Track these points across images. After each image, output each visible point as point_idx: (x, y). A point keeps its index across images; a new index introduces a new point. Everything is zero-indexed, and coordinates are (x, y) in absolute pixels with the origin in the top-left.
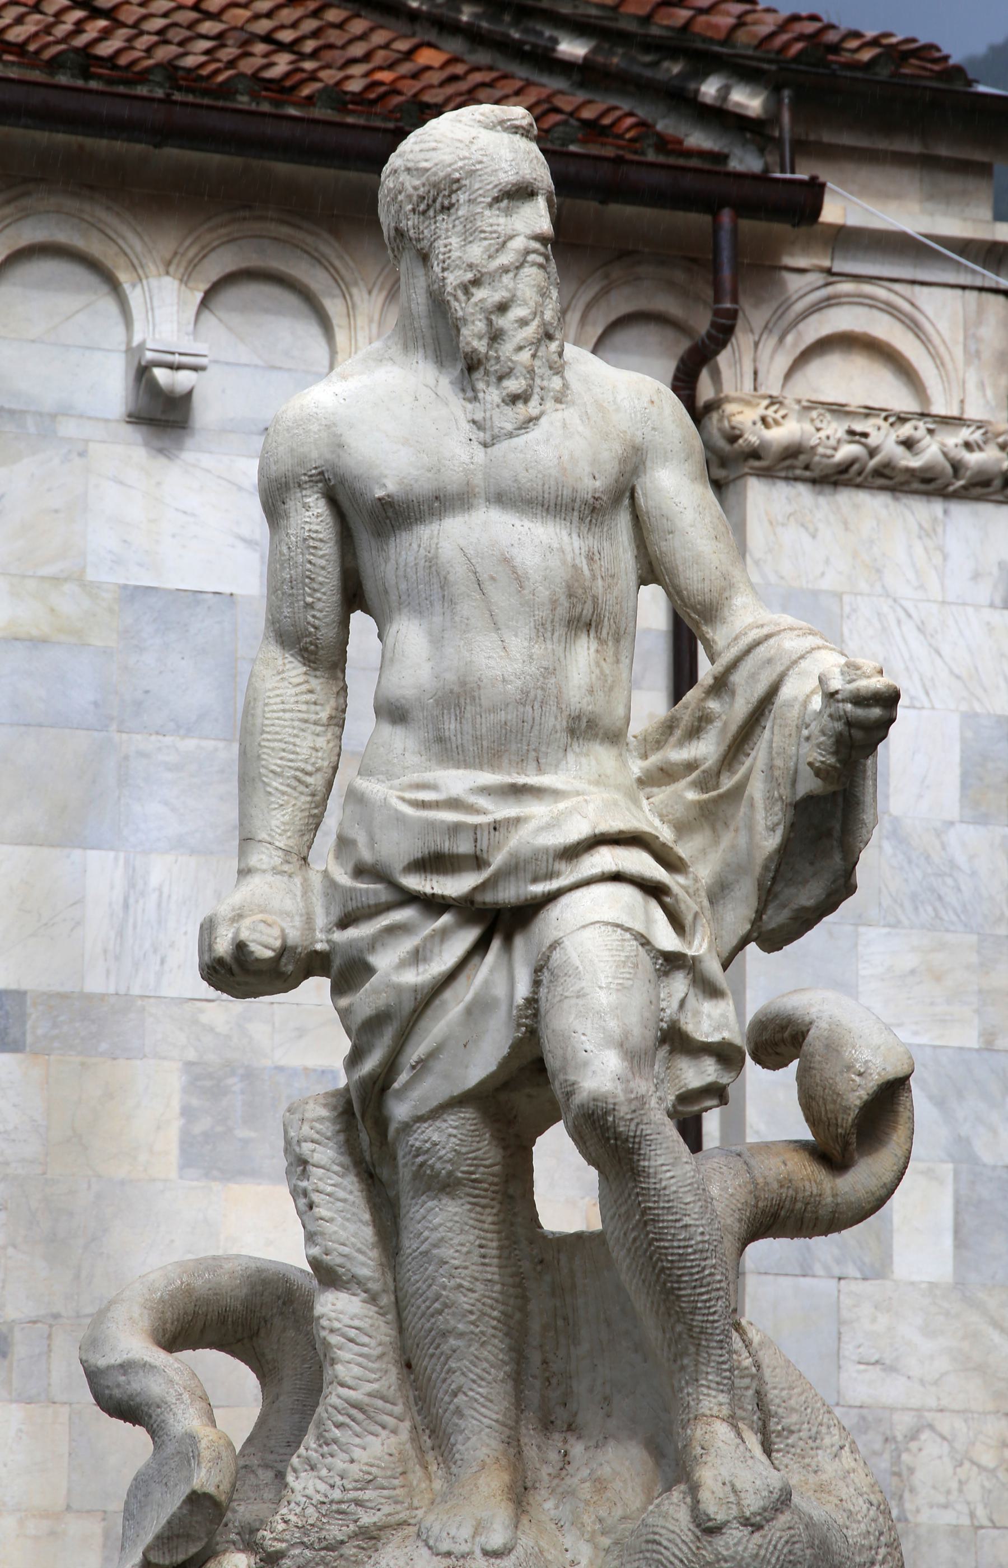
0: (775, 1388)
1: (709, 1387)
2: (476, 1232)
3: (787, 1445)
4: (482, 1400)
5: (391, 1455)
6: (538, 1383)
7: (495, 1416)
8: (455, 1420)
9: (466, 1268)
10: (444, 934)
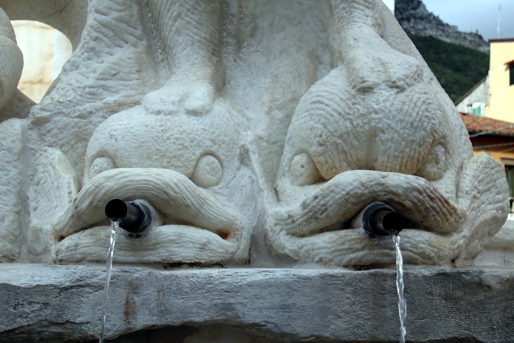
4: (194, 23)
5: (130, 59)
6: (235, 21)
7: (203, 35)
8: (176, 37)
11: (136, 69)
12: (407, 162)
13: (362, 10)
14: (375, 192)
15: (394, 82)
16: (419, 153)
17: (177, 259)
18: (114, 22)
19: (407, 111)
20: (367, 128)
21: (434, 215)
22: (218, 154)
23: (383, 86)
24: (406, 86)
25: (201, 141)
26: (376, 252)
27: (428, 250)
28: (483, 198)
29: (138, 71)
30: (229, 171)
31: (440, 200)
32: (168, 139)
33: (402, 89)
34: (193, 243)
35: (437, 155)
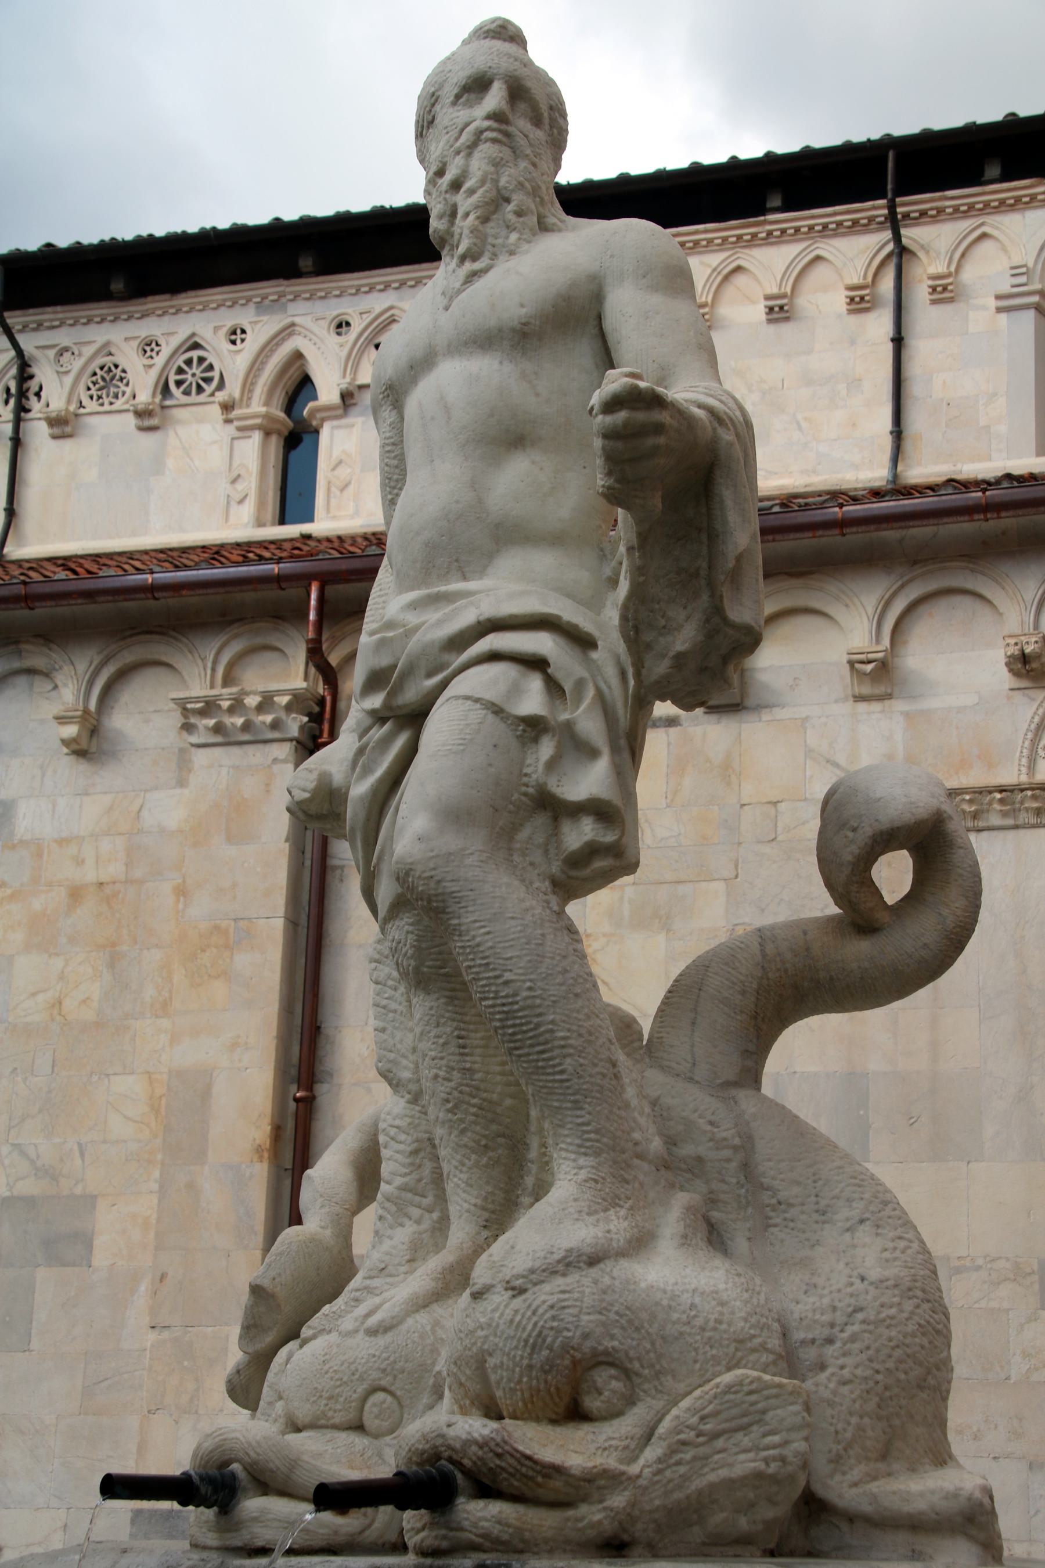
0: (770, 1160)
1: (567, 1150)
2: (455, 1024)
3: (785, 1219)
7: (473, 1201)
9: (442, 1058)
10: (385, 742)
11: (407, 1258)
12: (532, 1396)
13: (574, 1160)
14: (436, 1447)
15: (508, 1282)
16: (546, 1381)
17: (259, 1543)
18: (396, 1193)
19: (520, 1322)
20: (474, 1349)
21: (506, 1479)
22: (393, 1388)
23: (499, 1288)
24: (529, 1286)
25: (365, 1372)
26: (434, 1533)
27: (496, 1530)
28: (720, 1443)
29: (409, 1261)
30: (413, 1411)
31: (512, 1456)
32: (327, 1373)
33: (522, 1291)
34: (280, 1521)
35: (594, 1382)
